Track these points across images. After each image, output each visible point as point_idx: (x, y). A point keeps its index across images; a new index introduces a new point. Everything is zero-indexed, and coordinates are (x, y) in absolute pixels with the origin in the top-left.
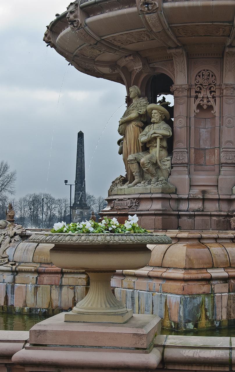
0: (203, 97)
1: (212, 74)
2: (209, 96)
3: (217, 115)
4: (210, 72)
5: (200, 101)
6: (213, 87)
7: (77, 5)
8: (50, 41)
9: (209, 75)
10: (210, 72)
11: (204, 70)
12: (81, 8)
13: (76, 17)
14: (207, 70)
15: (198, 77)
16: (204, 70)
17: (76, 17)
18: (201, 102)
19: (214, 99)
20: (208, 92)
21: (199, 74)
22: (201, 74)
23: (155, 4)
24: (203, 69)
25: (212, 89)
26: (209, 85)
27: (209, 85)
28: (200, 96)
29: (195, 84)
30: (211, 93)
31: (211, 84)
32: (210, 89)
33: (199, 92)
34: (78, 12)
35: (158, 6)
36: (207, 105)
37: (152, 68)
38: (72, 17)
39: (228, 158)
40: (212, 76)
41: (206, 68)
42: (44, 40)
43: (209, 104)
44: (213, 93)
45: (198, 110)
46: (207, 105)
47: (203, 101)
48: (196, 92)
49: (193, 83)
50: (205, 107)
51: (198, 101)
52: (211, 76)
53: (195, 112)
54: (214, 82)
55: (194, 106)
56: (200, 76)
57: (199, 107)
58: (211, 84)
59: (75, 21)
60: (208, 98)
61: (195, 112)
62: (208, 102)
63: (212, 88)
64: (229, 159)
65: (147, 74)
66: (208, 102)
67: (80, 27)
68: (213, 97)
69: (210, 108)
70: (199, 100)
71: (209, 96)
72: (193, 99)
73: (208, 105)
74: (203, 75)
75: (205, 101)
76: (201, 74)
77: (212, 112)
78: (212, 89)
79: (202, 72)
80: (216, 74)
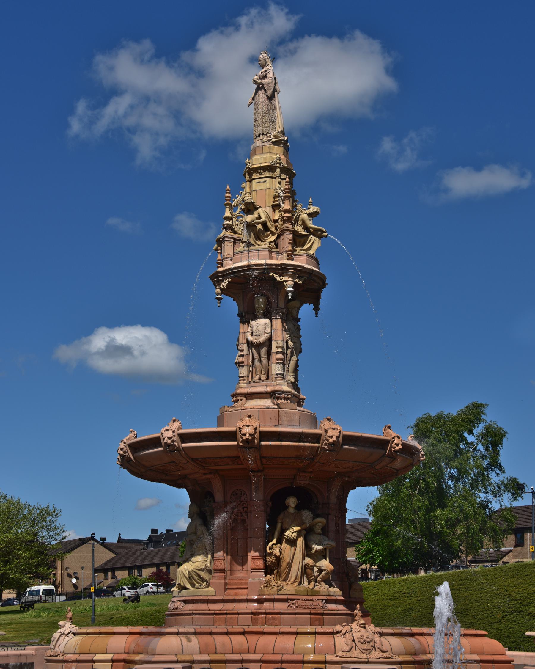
2: (242, 511)
6: (245, 503)
14: (240, 490)
16: (237, 490)
30: (243, 509)
31: (243, 501)
32: (243, 505)
40: (244, 494)
43: (242, 518)
52: (243, 494)
54: (245, 500)
56: (234, 495)
58: (243, 501)
63: (244, 505)
68: (246, 512)
74: (236, 494)
78: (244, 505)
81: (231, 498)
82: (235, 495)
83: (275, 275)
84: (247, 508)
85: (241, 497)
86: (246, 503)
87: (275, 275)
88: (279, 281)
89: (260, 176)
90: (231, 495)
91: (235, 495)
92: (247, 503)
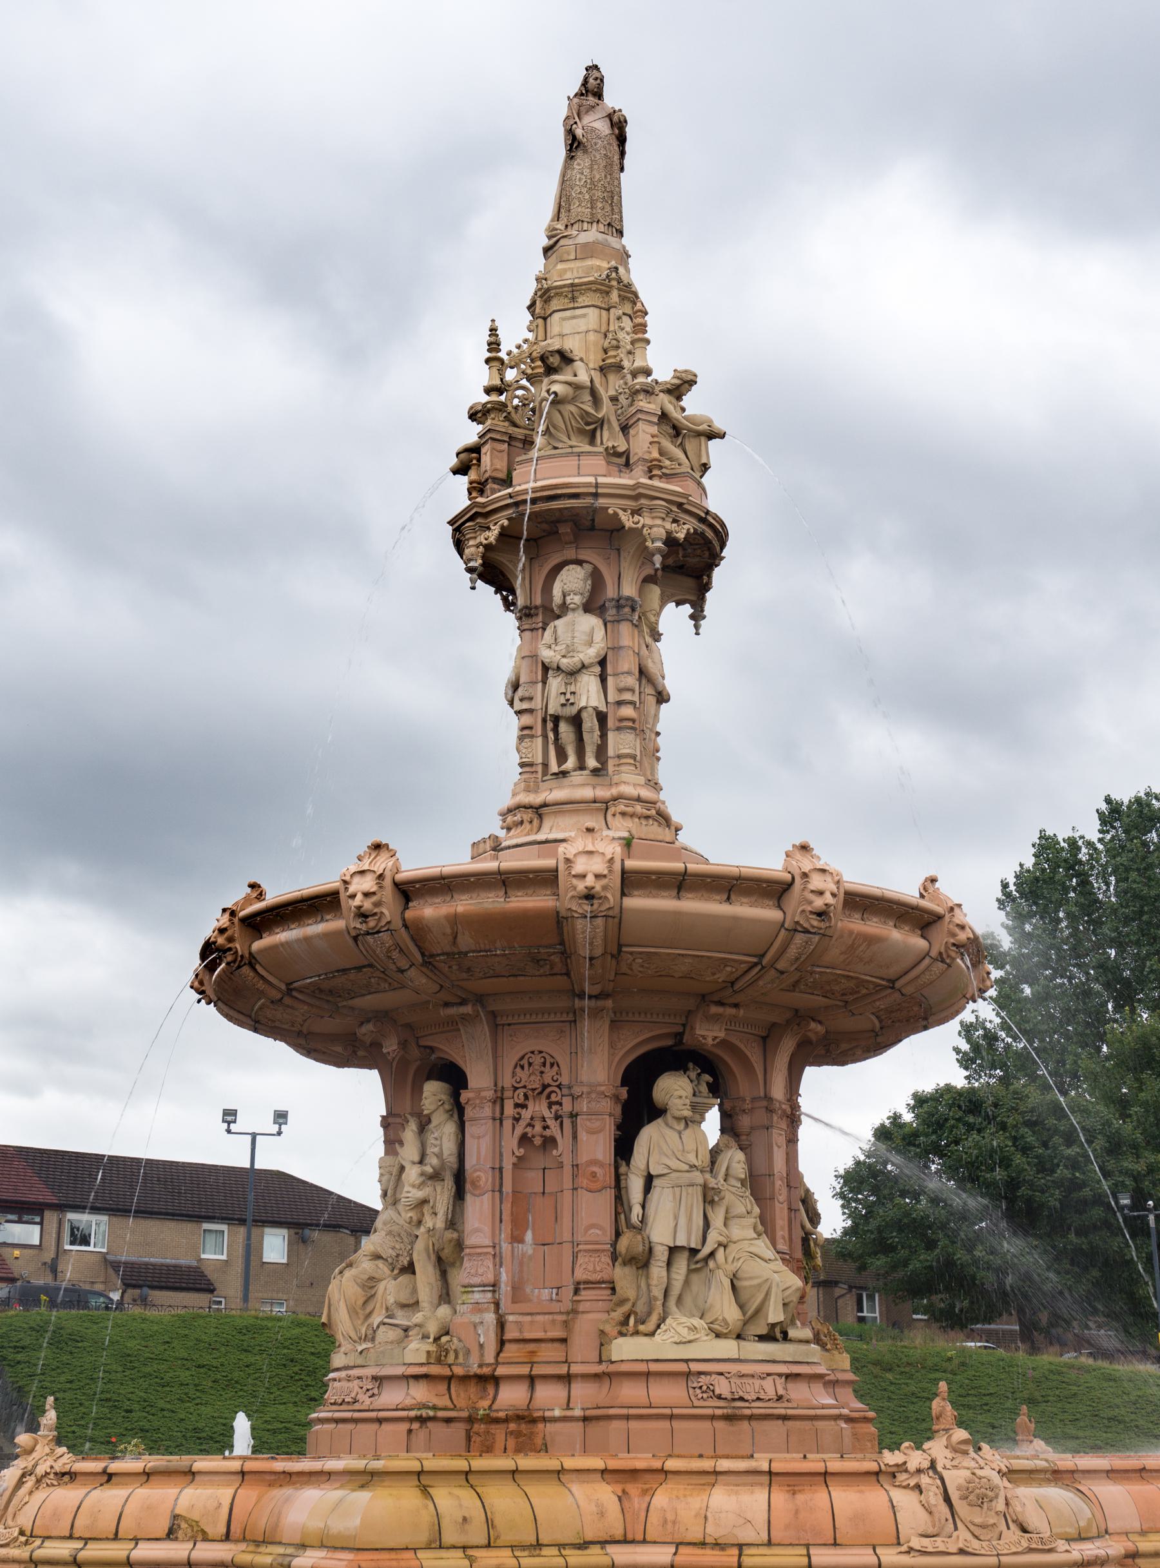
0: (532, 1118)
1: (552, 1061)
2: (547, 1114)
3: (567, 1160)
4: (548, 1057)
5: (526, 1127)
7: (233, 913)
8: (203, 988)
9: (544, 1064)
10: (548, 1057)
11: (533, 1052)
12: (243, 920)
13: (230, 940)
14: (541, 1052)
15: (518, 1069)
16: (533, 1052)
17: (230, 940)
18: (529, 1129)
19: (558, 1121)
20: (544, 1104)
21: (522, 1063)
22: (525, 1062)
23: (382, 913)
24: (532, 1049)
25: (553, 1098)
26: (545, 1087)
27: (545, 1087)
28: (526, 1114)
29: (513, 1086)
30: (550, 1107)
31: (549, 1085)
32: (548, 1097)
33: (524, 1106)
34: (236, 931)
35: (389, 919)
36: (542, 1136)
37: (426, 1047)
38: (221, 940)
39: (591, 1268)
40: (552, 1065)
41: (537, 1048)
42: (192, 987)
43: (548, 1133)
44: (555, 1108)
45: (522, 1150)
46: (542, 1136)
47: (533, 1126)
48: (517, 1105)
49: (507, 1081)
50: (538, 1141)
51: (519, 1131)
52: (548, 1065)
53: (513, 1153)
55: (511, 1142)
56: (522, 1067)
57: (524, 1139)
59: (230, 949)
60: (544, 1119)
61: (513, 1153)
62: (545, 1128)
63: (553, 1095)
64: (595, 1271)
65: (418, 1063)
66: (545, 1128)
67: (241, 961)
68: (557, 1117)
69: (549, 1142)
70: (523, 1123)
71: (547, 1114)
72: (508, 1124)
73: (544, 1137)
74: (530, 1064)
75: (538, 1128)
76: (525, 1062)
77: (554, 1152)
78: (553, 1098)
79: (527, 1057)
80: (559, 1059)
81: (514, 1074)
82: (526, 1066)
83: (621, 513)
84: (561, 1104)
85: (542, 1072)
86: (557, 1090)
87: (621, 513)
88: (631, 529)
89: (571, 305)
90: (515, 1067)
91: (526, 1066)
92: (560, 1089)
